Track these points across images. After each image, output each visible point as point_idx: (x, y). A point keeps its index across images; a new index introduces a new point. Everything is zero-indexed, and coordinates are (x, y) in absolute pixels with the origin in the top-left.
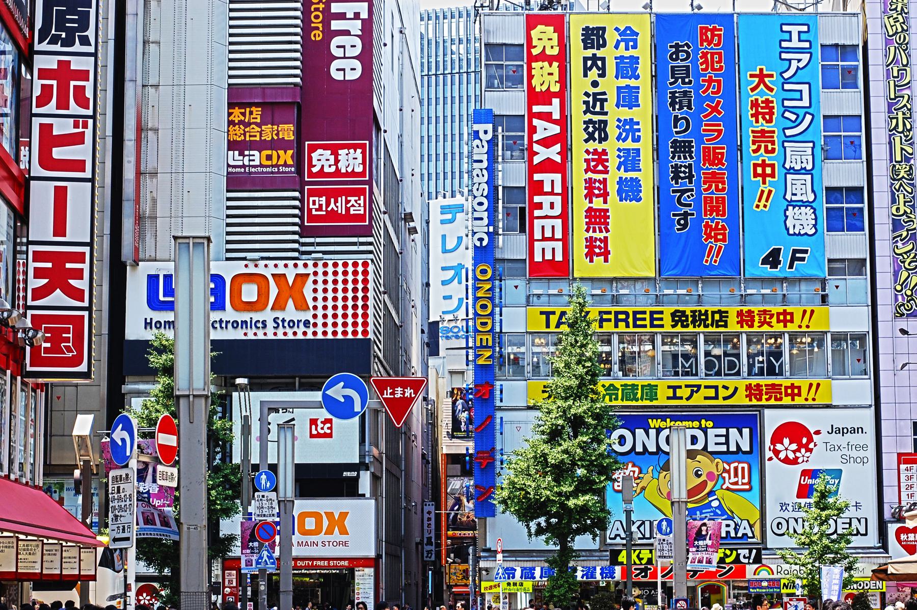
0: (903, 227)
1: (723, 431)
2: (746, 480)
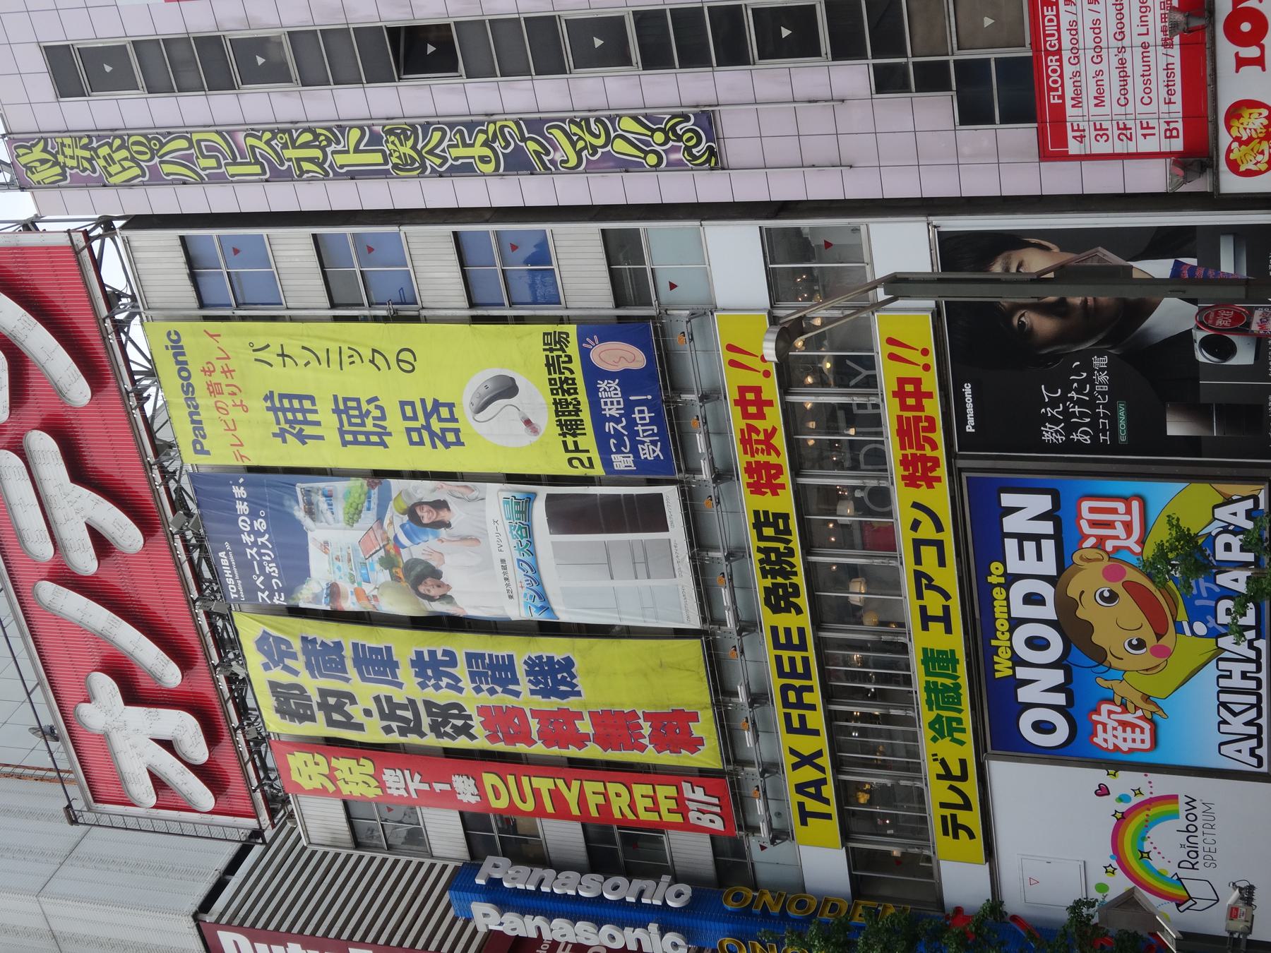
1: (1011, 545)
2: (1121, 506)
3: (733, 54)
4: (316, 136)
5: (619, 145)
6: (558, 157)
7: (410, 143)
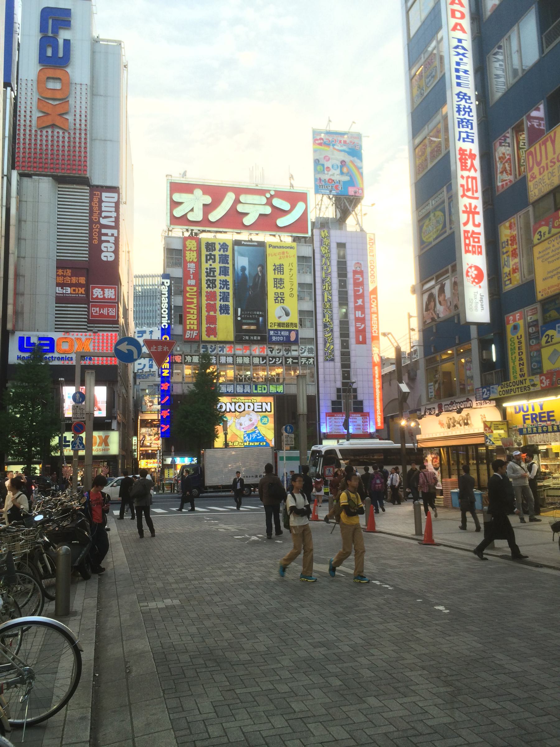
3: (343, 366)
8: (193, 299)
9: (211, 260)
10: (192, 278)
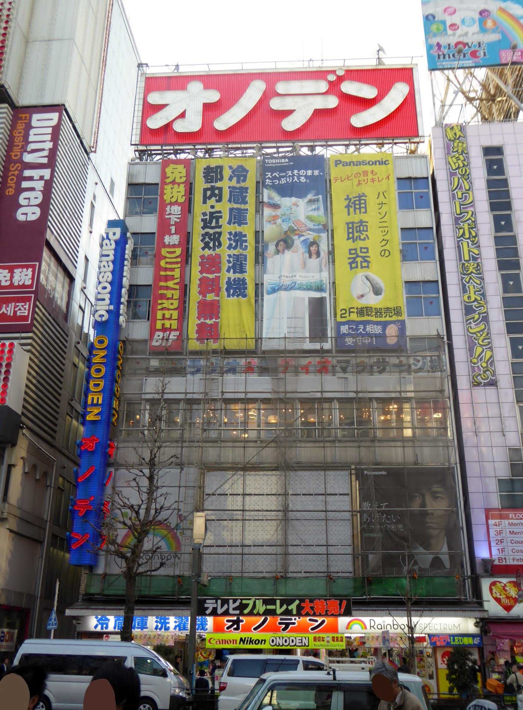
0: (476, 311)
4: (475, 237)
5: (479, 350)
6: (473, 325)
7: (474, 271)
8: (172, 270)
9: (213, 199)
10: (173, 231)
